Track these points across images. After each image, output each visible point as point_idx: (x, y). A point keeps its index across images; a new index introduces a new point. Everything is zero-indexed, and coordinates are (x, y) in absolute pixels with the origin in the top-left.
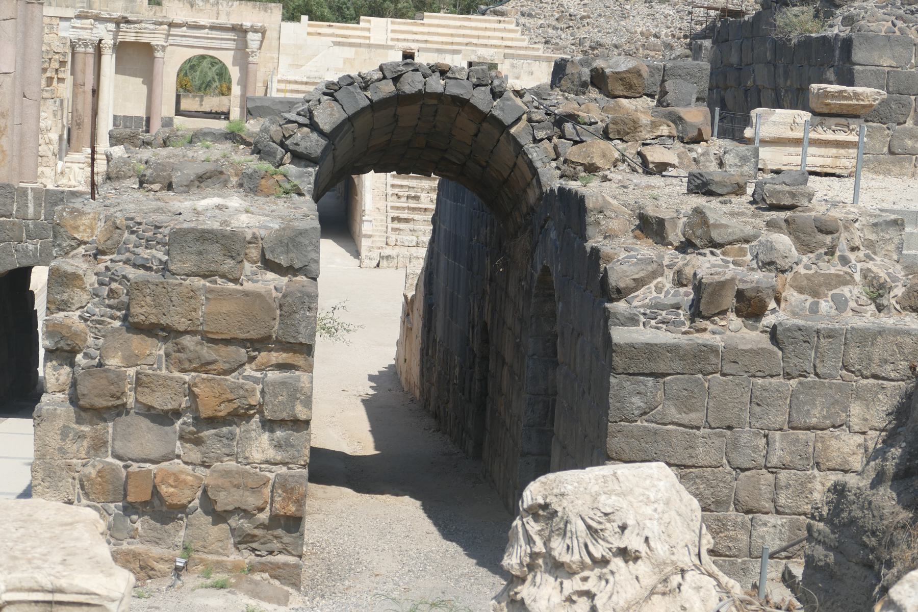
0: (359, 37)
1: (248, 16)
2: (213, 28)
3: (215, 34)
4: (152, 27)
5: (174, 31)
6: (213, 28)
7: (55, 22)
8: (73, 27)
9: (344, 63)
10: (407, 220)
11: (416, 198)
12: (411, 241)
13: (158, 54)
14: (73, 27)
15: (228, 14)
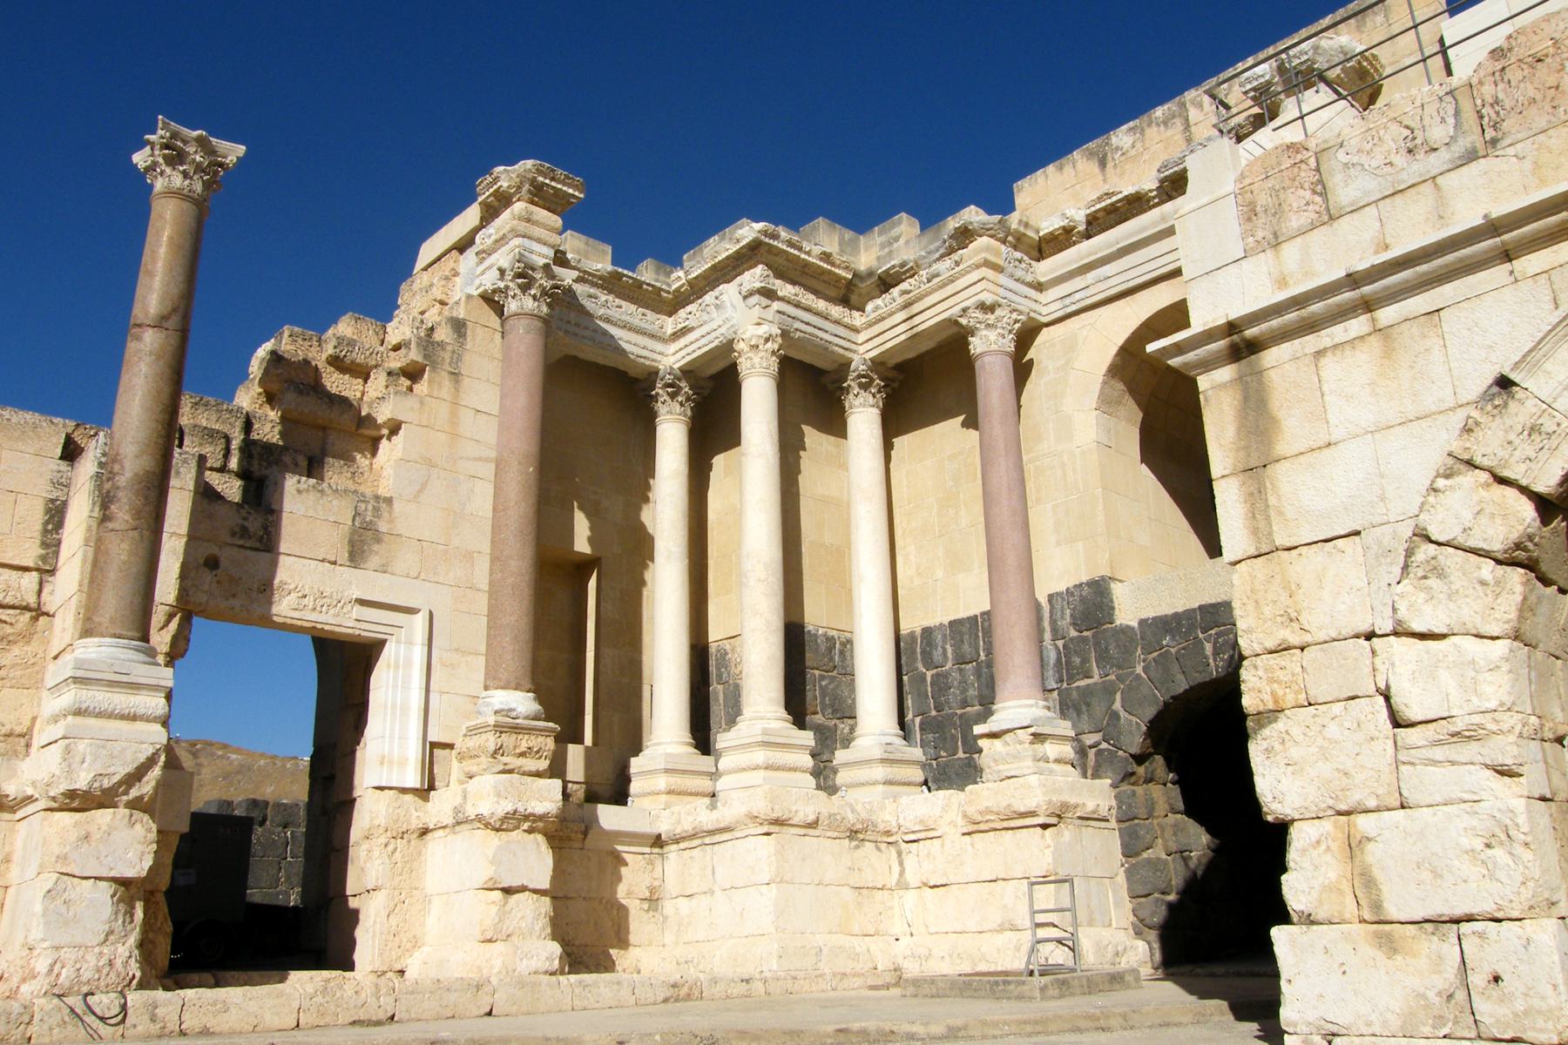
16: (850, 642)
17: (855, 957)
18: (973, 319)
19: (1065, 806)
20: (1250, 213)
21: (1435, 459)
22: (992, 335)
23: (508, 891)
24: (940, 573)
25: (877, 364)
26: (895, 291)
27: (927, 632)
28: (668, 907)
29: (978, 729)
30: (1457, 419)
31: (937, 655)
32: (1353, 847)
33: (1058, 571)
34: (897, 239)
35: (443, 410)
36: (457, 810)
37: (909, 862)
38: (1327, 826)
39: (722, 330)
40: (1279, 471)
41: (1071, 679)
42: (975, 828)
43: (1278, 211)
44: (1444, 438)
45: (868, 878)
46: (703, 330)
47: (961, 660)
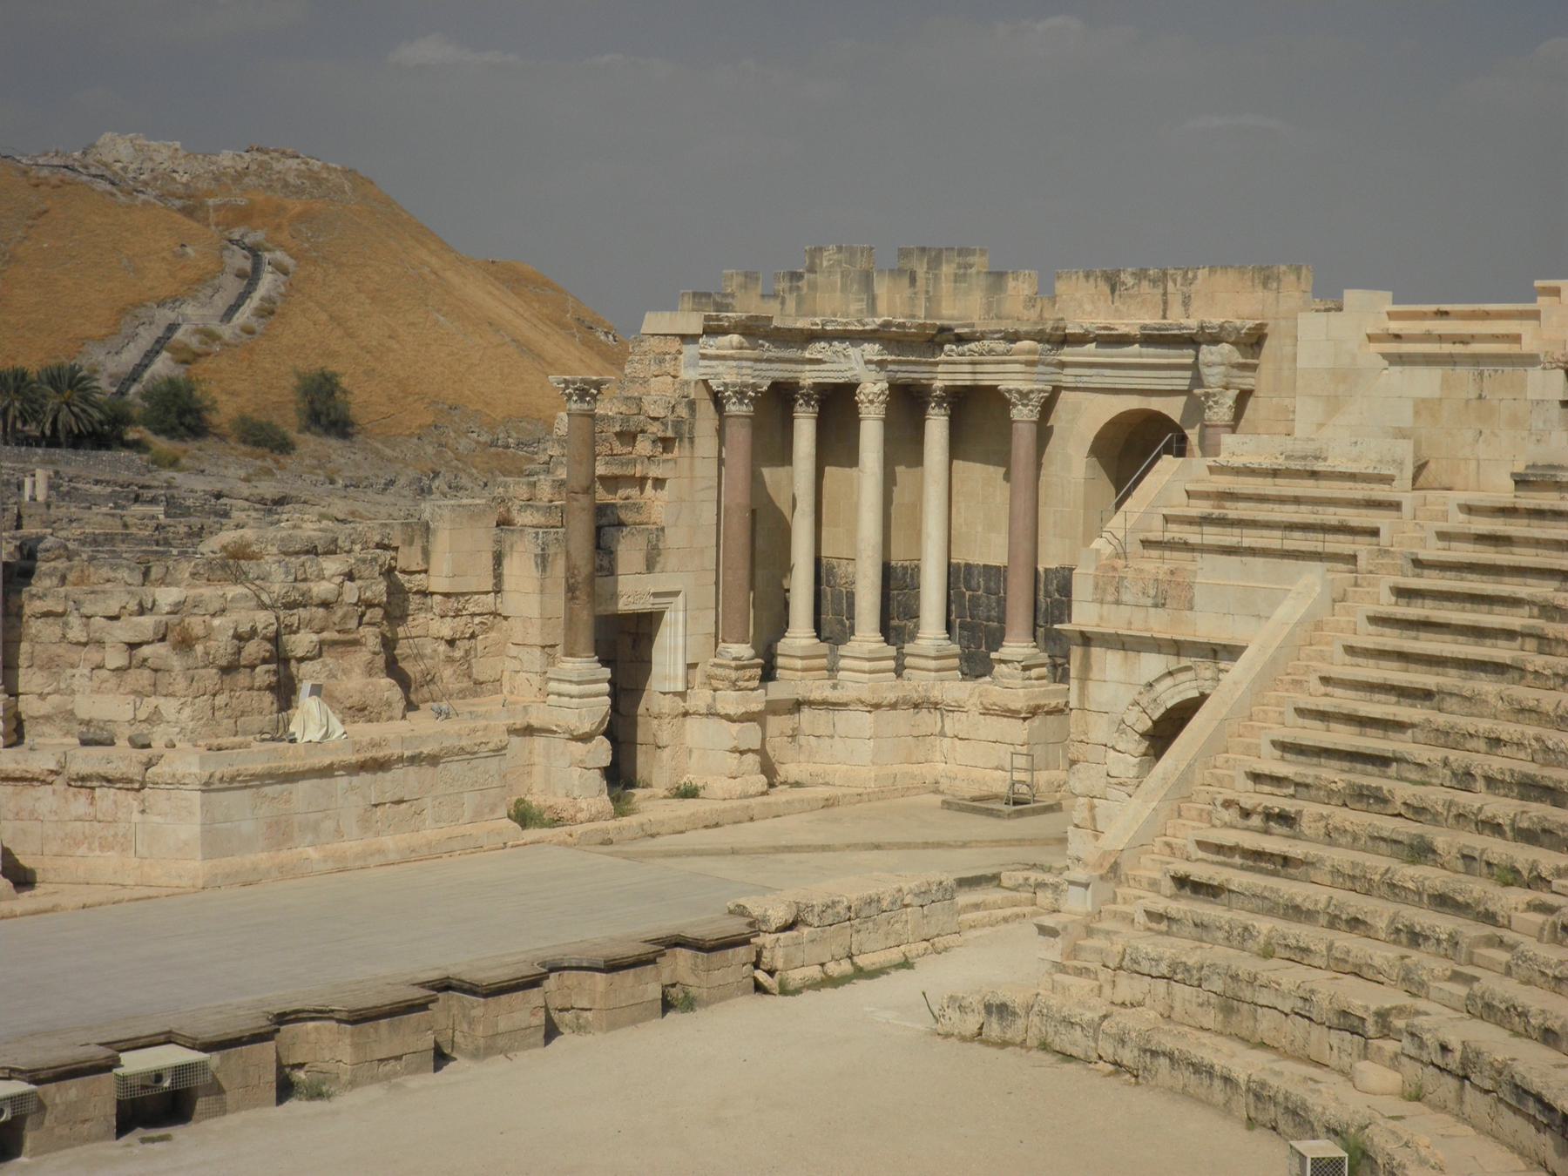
0: (1496, 338)
1: (1222, 301)
2: (1151, 339)
3: (1152, 355)
4: (1001, 346)
5: (1068, 354)
6: (1151, 339)
7: (676, 344)
8: (704, 357)
9: (1417, 413)
10: (1210, 891)
11: (1285, 819)
12: (1158, 961)
13: (1023, 414)
14: (704, 357)
15: (1186, 302)
16: (917, 567)
17: (914, 777)
18: (1014, 398)
19: (1038, 707)
20: (1096, 587)
21: (1130, 699)
22: (1025, 411)
23: (742, 753)
24: (980, 529)
25: (946, 389)
26: (966, 347)
27: (968, 566)
28: (802, 740)
29: (993, 655)
30: (1139, 688)
31: (974, 583)
32: (1092, 808)
33: (1049, 560)
34: (971, 266)
35: (685, 463)
36: (709, 706)
37: (948, 722)
38: (1086, 800)
39: (849, 374)
40: (1090, 684)
41: (1053, 623)
42: (986, 712)
43: (1104, 591)
44: (1133, 694)
45: (923, 730)
46: (834, 367)
47: (988, 591)
